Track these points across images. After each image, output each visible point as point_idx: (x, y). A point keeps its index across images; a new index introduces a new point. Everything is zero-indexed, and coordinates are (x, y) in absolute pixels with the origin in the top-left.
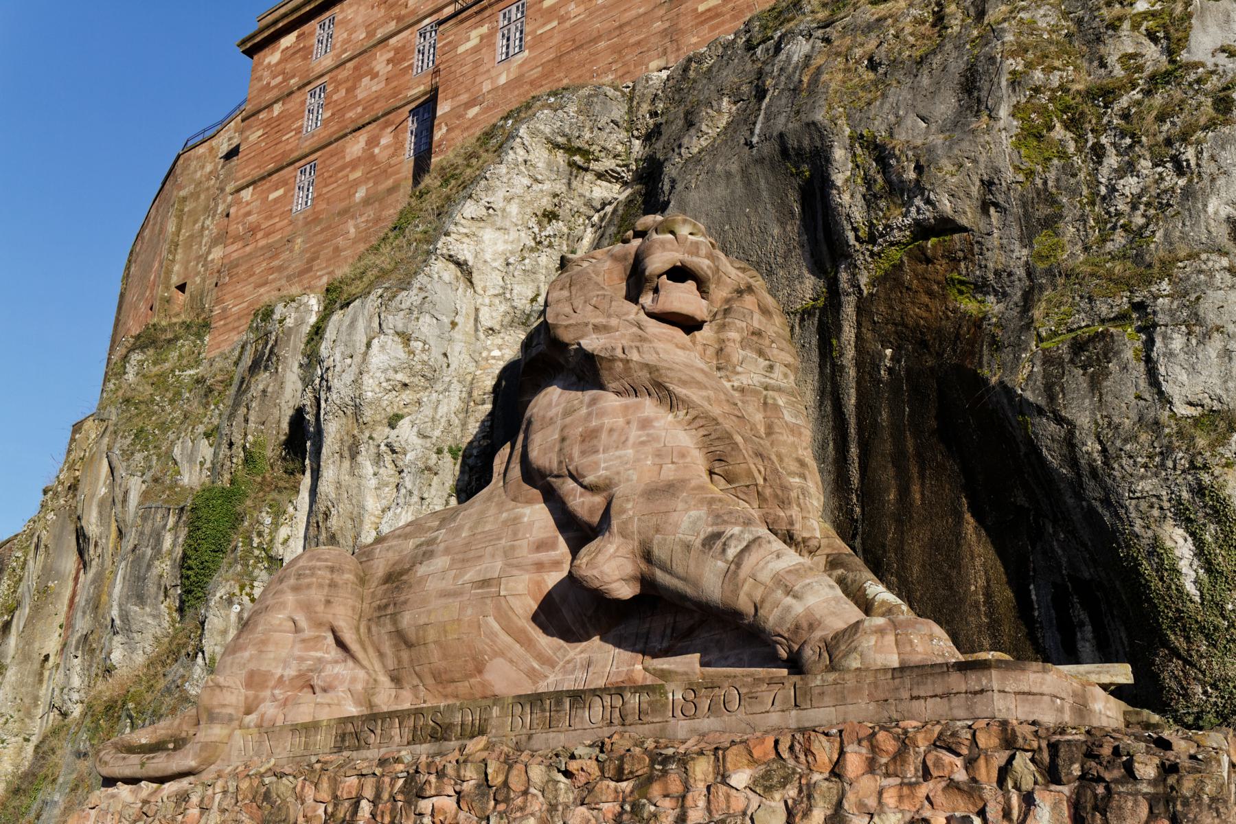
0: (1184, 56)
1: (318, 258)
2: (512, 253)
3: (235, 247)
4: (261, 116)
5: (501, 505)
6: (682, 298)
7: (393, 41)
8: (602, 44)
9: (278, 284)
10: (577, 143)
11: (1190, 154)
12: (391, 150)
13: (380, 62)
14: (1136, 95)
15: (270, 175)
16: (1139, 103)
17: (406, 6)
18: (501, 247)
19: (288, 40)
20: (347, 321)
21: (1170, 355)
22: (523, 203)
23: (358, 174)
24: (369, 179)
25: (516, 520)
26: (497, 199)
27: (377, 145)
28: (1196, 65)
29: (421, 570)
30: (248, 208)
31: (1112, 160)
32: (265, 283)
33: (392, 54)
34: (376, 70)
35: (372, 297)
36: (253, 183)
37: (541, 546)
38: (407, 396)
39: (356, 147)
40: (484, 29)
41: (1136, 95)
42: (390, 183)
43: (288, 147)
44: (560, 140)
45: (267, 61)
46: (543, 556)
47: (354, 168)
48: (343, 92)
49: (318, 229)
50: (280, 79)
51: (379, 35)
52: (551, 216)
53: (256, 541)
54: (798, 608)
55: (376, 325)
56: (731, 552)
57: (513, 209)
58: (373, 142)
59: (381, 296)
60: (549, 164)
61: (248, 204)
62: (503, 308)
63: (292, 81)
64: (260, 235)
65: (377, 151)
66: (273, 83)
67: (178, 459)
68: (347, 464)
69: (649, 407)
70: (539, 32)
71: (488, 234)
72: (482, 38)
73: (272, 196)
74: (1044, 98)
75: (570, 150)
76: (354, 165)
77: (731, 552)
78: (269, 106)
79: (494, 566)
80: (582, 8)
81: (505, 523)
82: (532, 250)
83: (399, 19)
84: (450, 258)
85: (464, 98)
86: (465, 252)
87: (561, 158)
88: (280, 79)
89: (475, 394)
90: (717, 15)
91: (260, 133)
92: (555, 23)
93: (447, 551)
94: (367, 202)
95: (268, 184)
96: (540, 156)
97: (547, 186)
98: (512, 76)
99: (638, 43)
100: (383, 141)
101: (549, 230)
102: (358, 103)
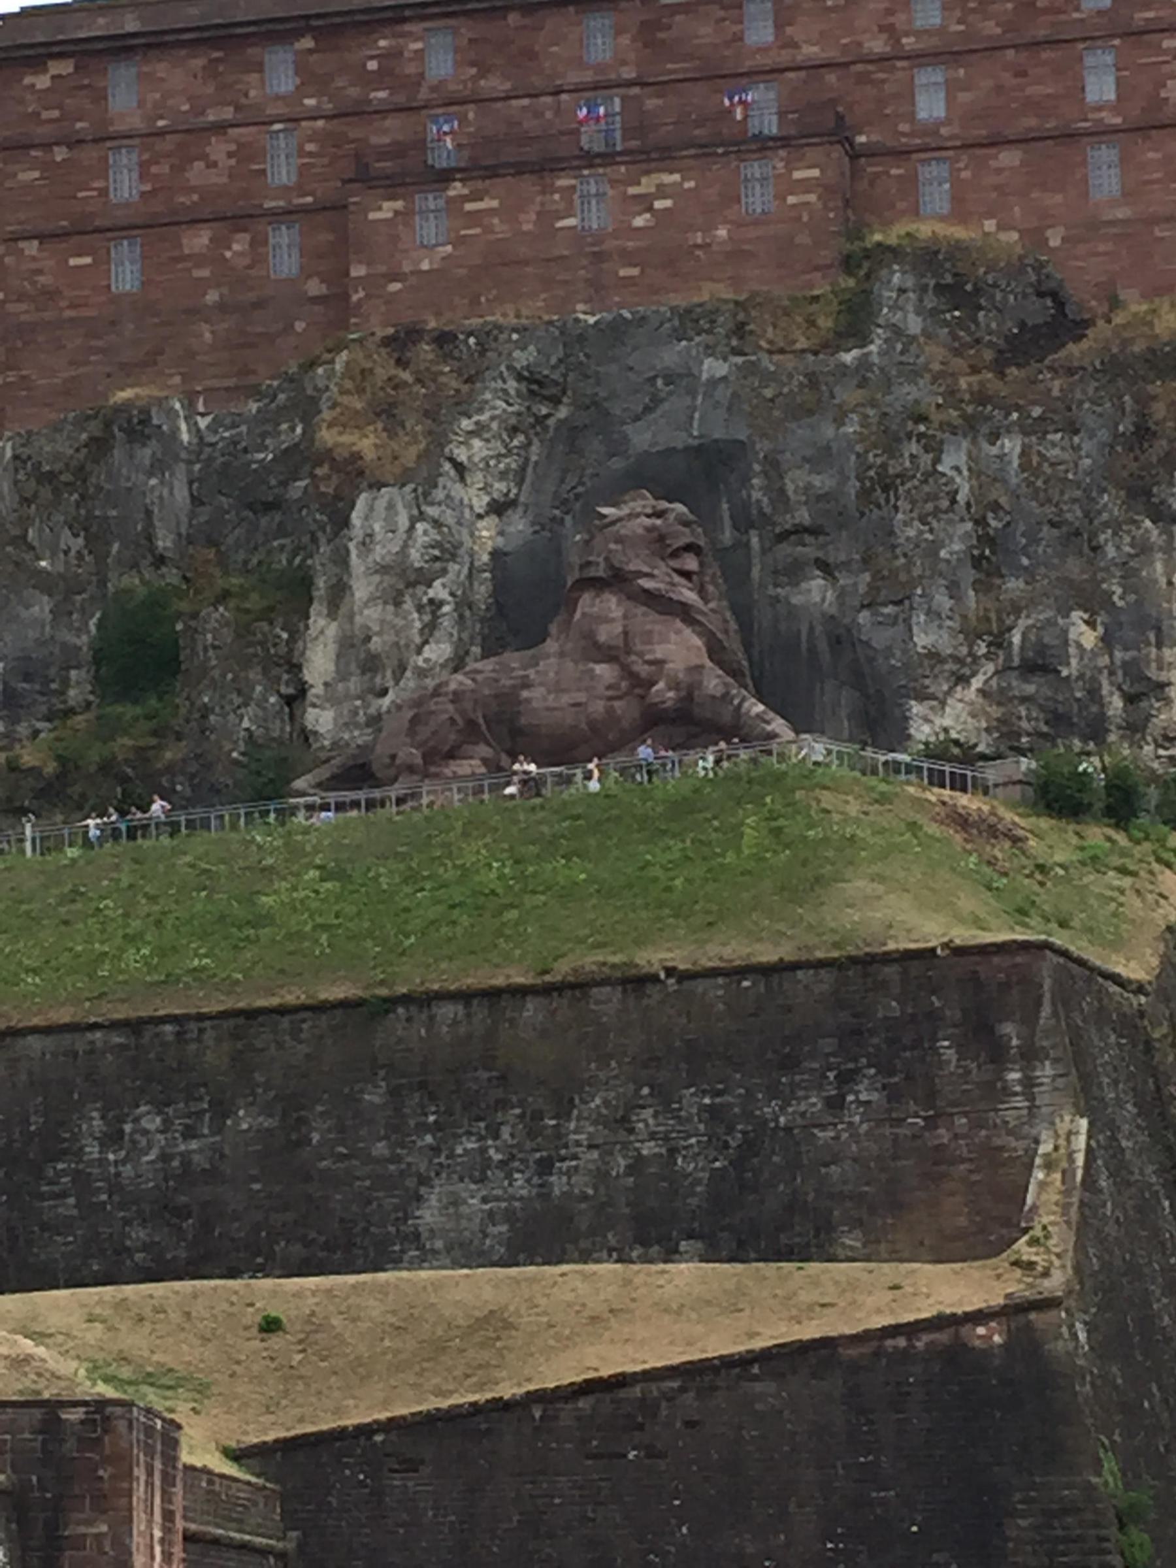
0: (940, 468)
1: (162, 353)
2: (492, 457)
3: (23, 307)
4: (33, 153)
5: (576, 662)
6: (691, 563)
7: (230, 131)
8: (529, 269)
9: (108, 369)
10: (538, 377)
11: (935, 524)
12: (247, 261)
13: (218, 149)
14: (916, 482)
15: (65, 234)
16: (916, 488)
17: (246, 95)
18: (486, 453)
19: (64, 67)
20: (381, 504)
21: (918, 623)
22: (502, 421)
23: (205, 273)
24: (218, 285)
25: (592, 670)
26: (484, 417)
27: (229, 248)
28: (944, 475)
29: (525, 694)
30: (34, 266)
31: (900, 516)
32: (87, 363)
33: (233, 147)
34: (213, 157)
35: (409, 488)
36: (41, 237)
37: (609, 687)
38: (438, 565)
39: (199, 240)
40: (399, 204)
41: (916, 482)
42: (252, 296)
43: (89, 209)
44: (526, 374)
45: (28, 80)
46: (610, 693)
47: (198, 266)
48: (166, 169)
49: (156, 320)
50: (56, 114)
51: (211, 117)
52: (514, 431)
53: (272, 651)
54: (769, 728)
55: (415, 512)
56: (736, 702)
57: (495, 425)
58: (221, 242)
59: (415, 490)
60: (518, 391)
61: (34, 259)
62: (486, 499)
63: (79, 125)
64: (63, 304)
65: (228, 254)
66: (45, 115)
67: (36, 544)
68: (390, 608)
69: (679, 624)
70: (463, 232)
71: (477, 443)
72: (396, 213)
73: (73, 262)
74: (872, 473)
75: (530, 381)
76: (199, 260)
77: (736, 702)
78: (47, 146)
79: (581, 697)
80: (505, 227)
81: (583, 672)
82: (505, 456)
83: (238, 108)
84: (452, 460)
85: (382, 269)
86: (462, 455)
87: (523, 387)
88: (56, 114)
89: (477, 564)
90: (635, 285)
91: (37, 174)
92: (478, 231)
93: (541, 684)
94: (222, 307)
95: (64, 245)
96: (512, 385)
97: (515, 408)
98: (435, 266)
99: (566, 282)
100: (236, 247)
101: (515, 443)
102: (193, 189)
